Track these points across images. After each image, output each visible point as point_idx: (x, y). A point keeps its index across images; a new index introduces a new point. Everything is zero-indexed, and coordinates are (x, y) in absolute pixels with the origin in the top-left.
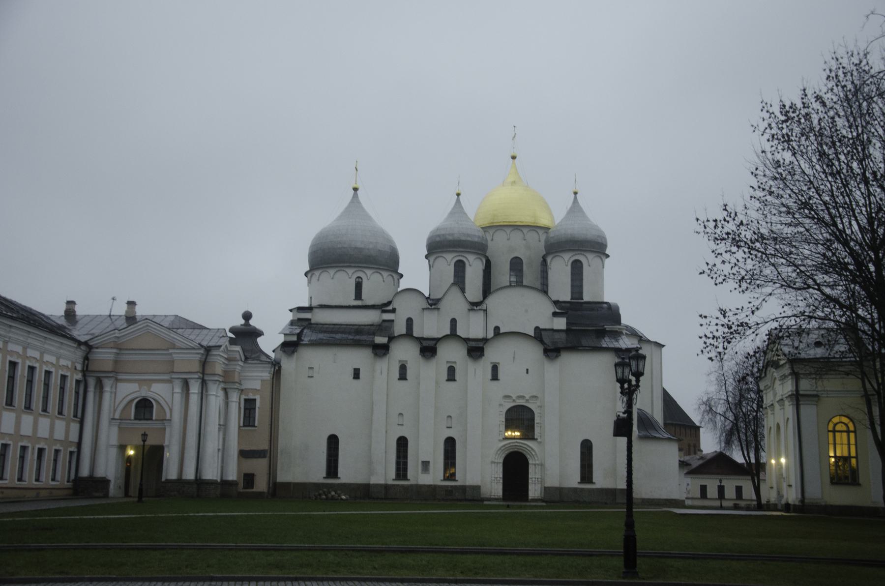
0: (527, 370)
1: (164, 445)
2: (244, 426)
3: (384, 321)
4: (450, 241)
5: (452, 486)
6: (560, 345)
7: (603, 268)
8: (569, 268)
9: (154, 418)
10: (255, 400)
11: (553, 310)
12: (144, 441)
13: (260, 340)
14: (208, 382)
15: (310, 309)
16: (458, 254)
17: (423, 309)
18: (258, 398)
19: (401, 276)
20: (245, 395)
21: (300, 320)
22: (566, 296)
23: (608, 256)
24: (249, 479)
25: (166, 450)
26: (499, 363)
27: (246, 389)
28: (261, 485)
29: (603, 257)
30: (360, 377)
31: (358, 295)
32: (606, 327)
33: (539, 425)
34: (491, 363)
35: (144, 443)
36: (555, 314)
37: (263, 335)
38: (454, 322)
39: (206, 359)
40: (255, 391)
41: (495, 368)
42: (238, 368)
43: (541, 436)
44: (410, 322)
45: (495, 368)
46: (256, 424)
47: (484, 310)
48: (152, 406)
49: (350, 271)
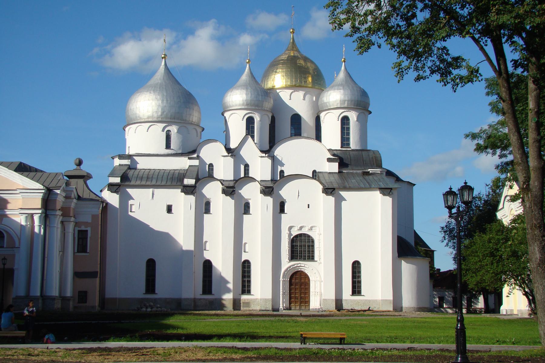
0: (309, 205)
1: (14, 268)
2: (78, 252)
5: (248, 299)
7: (367, 122)
8: (339, 123)
9: (5, 246)
10: (87, 231)
12: (4, 264)
13: (89, 182)
14: (49, 216)
15: (130, 157)
16: (249, 111)
18: (89, 229)
19: (203, 129)
20: (79, 227)
21: (120, 165)
22: (337, 145)
23: (370, 113)
24: (82, 296)
25: (16, 272)
27: (79, 222)
28: (94, 301)
29: (367, 113)
30: (173, 211)
31: (168, 146)
32: (369, 170)
33: (318, 249)
35: (4, 266)
36: (329, 160)
37: (92, 178)
39: (48, 197)
40: (86, 224)
42: (73, 205)
43: (320, 259)
46: (88, 251)
48: (4, 237)
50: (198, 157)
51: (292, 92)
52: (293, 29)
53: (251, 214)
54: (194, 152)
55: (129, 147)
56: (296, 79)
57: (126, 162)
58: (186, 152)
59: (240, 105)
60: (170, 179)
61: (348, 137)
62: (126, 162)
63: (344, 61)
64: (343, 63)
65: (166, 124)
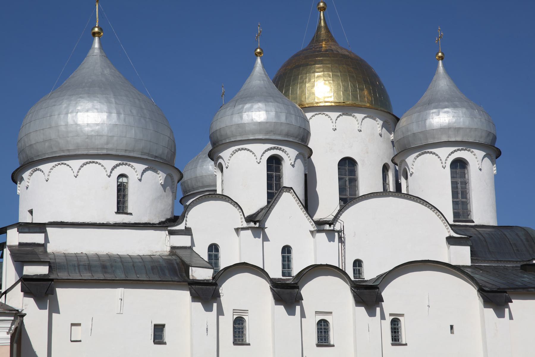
0: (452, 327)
3: (173, 248)
4: (260, 123)
6: (502, 286)
11: (448, 235)
15: (40, 228)
17: (237, 230)
21: (21, 244)
26: (402, 315)
34: (391, 315)
38: (286, 250)
41: (395, 324)
44: (214, 248)
45: (395, 324)
47: (339, 232)
49: (110, 163)
50: (188, 231)
51: (340, 115)
52: (325, 3)
53: (333, 346)
54: (175, 220)
55: (31, 212)
56: (345, 90)
57: (37, 238)
58: (156, 220)
59: (253, 133)
60: (153, 268)
61: (464, 200)
62: (37, 238)
63: (442, 58)
64: (440, 62)
65: (118, 162)
